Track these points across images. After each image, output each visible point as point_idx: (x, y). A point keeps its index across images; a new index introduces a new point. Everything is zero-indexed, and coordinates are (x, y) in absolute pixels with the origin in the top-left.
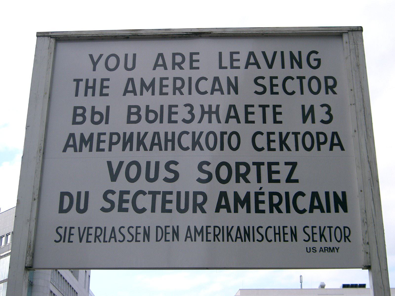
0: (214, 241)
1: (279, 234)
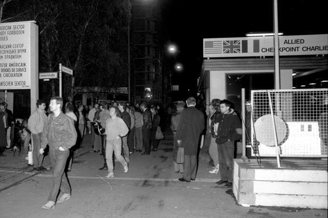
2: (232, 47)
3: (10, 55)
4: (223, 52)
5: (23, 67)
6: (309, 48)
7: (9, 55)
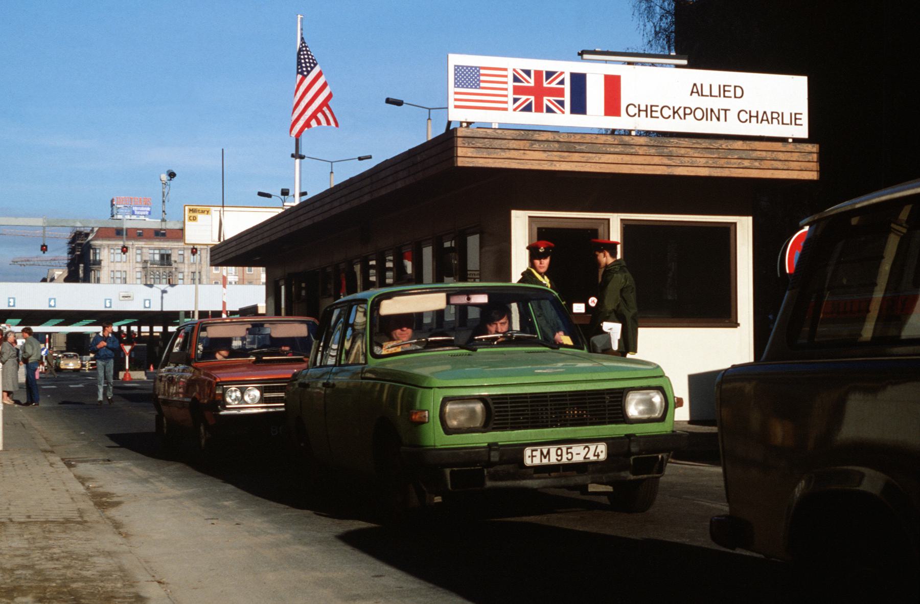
2: (539, 91)
4: (511, 106)
6: (754, 114)
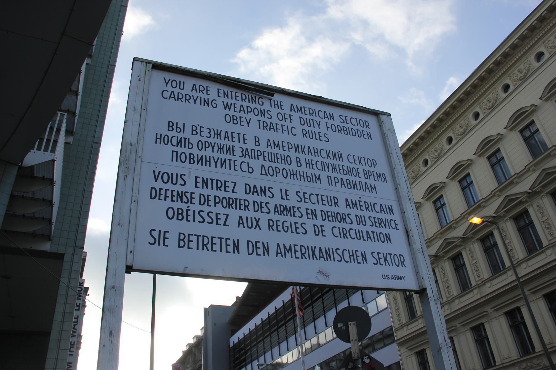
0: (302, 258)
1: (353, 255)
3: (345, 177)
5: (389, 217)
7: (339, 176)
